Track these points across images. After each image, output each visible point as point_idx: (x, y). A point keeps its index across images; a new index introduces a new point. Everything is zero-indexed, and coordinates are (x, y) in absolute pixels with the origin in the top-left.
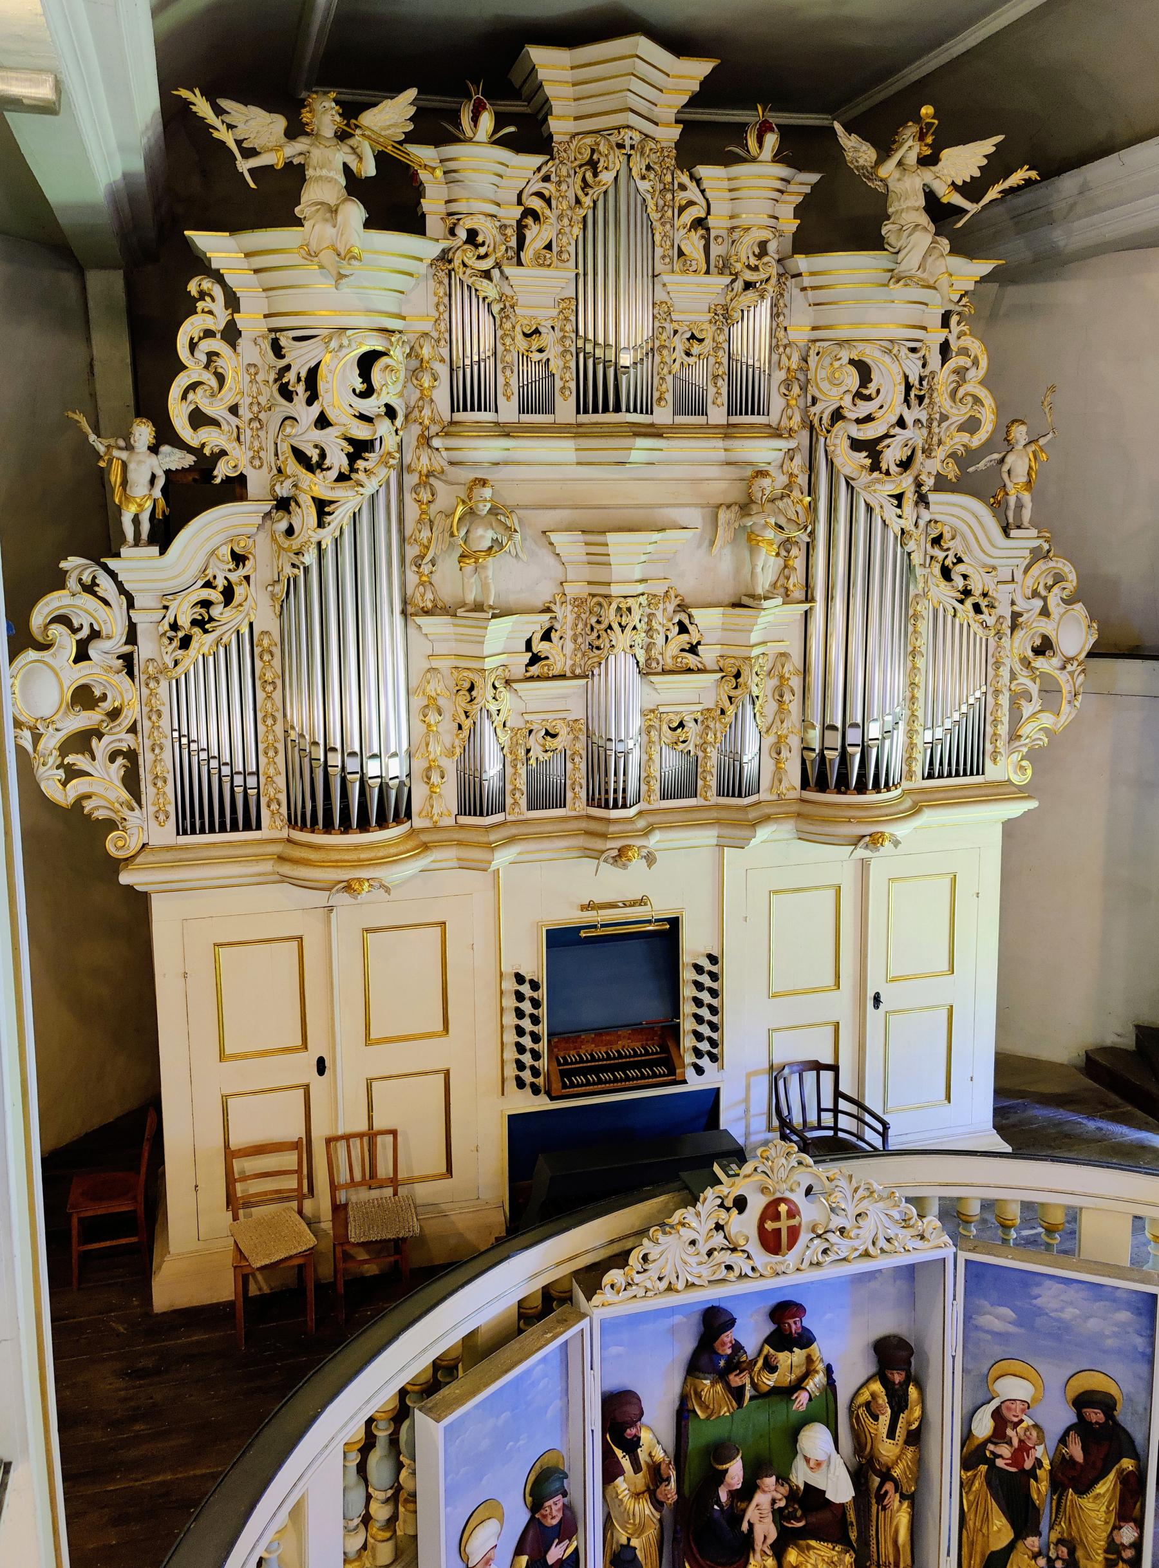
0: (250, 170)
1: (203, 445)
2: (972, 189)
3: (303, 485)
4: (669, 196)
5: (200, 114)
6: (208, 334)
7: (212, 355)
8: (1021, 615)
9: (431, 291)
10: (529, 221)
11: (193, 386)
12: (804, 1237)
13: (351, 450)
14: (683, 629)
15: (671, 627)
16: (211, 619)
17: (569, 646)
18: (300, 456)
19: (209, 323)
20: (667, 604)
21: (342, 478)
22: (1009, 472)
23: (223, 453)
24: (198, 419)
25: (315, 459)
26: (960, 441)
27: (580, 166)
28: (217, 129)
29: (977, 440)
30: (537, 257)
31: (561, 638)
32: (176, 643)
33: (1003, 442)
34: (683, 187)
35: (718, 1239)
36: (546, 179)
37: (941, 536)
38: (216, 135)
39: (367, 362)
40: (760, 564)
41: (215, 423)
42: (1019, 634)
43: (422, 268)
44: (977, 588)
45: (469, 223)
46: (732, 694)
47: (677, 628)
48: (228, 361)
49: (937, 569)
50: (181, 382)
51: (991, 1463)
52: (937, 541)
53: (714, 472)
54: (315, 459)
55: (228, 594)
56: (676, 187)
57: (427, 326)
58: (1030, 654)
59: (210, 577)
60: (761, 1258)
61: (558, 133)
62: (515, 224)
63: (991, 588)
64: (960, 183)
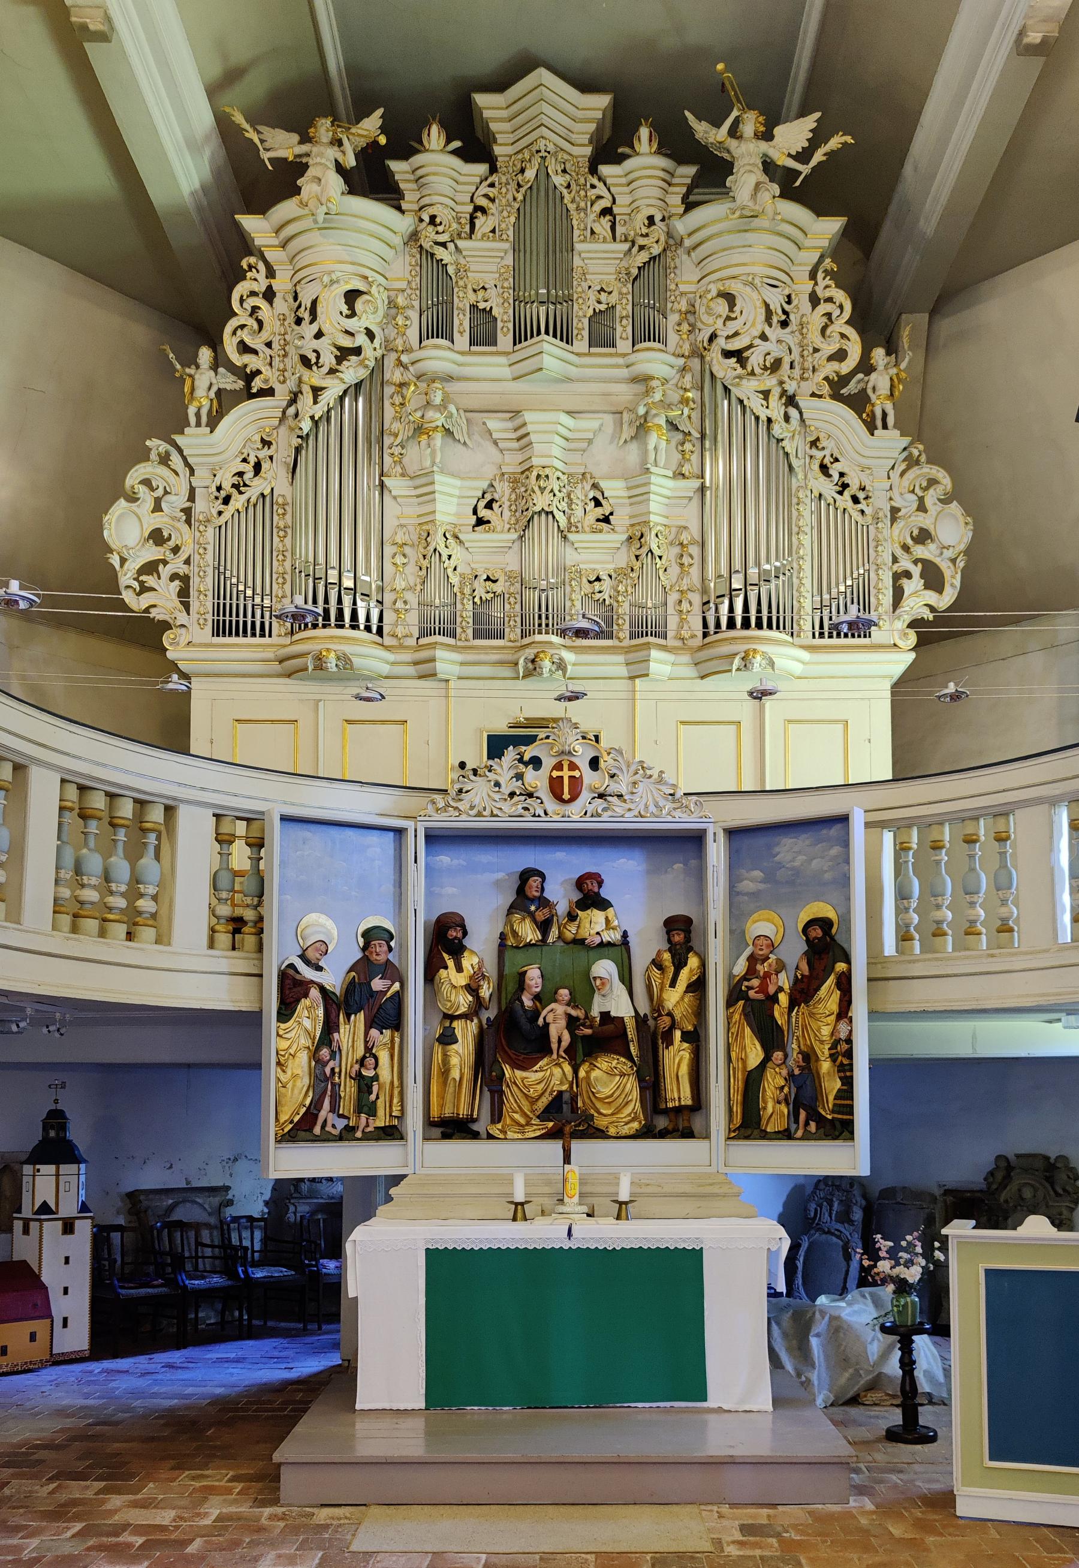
0: (269, 159)
1: (246, 366)
2: (803, 156)
3: (305, 378)
4: (582, 193)
5: (237, 122)
6: (253, 294)
7: (255, 309)
8: (899, 510)
9: (407, 263)
10: (479, 214)
11: (242, 327)
12: (585, 796)
13: (339, 354)
14: (598, 503)
15: (588, 502)
16: (245, 485)
17: (507, 514)
18: (305, 361)
19: (255, 287)
20: (585, 483)
21: (332, 371)
22: (874, 389)
23: (258, 372)
24: (244, 348)
25: (314, 360)
26: (830, 369)
27: (516, 175)
28: (247, 132)
29: (846, 367)
30: (484, 235)
31: (500, 506)
32: (220, 501)
33: (866, 367)
34: (593, 187)
35: (516, 785)
36: (492, 185)
37: (818, 439)
38: (247, 135)
39: (352, 296)
40: (651, 447)
41: (255, 352)
42: (899, 525)
43: (397, 241)
44: (854, 483)
45: (432, 211)
46: (637, 553)
47: (593, 503)
48: (265, 311)
49: (816, 467)
50: (233, 323)
51: (747, 999)
52: (814, 444)
53: (623, 388)
54: (314, 360)
55: (257, 468)
56: (588, 186)
57: (403, 285)
58: (909, 542)
59: (245, 455)
60: (551, 805)
61: (501, 156)
62: (468, 216)
63: (867, 483)
64: (794, 153)
